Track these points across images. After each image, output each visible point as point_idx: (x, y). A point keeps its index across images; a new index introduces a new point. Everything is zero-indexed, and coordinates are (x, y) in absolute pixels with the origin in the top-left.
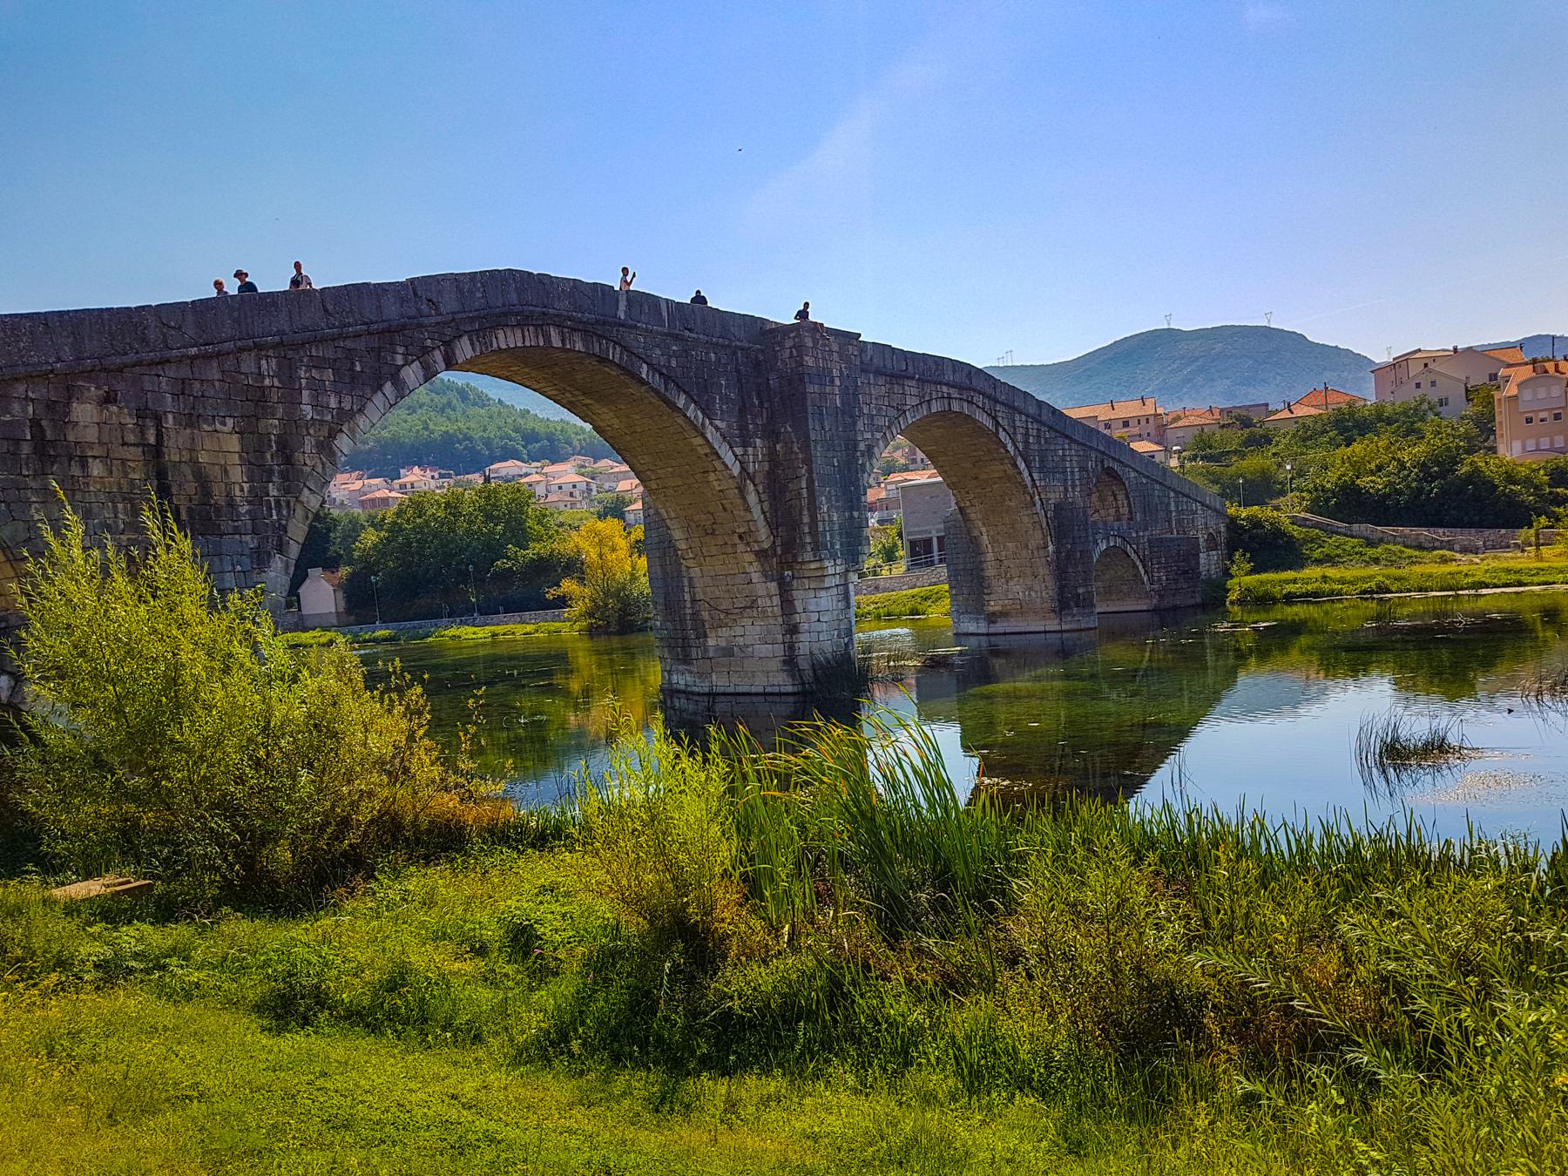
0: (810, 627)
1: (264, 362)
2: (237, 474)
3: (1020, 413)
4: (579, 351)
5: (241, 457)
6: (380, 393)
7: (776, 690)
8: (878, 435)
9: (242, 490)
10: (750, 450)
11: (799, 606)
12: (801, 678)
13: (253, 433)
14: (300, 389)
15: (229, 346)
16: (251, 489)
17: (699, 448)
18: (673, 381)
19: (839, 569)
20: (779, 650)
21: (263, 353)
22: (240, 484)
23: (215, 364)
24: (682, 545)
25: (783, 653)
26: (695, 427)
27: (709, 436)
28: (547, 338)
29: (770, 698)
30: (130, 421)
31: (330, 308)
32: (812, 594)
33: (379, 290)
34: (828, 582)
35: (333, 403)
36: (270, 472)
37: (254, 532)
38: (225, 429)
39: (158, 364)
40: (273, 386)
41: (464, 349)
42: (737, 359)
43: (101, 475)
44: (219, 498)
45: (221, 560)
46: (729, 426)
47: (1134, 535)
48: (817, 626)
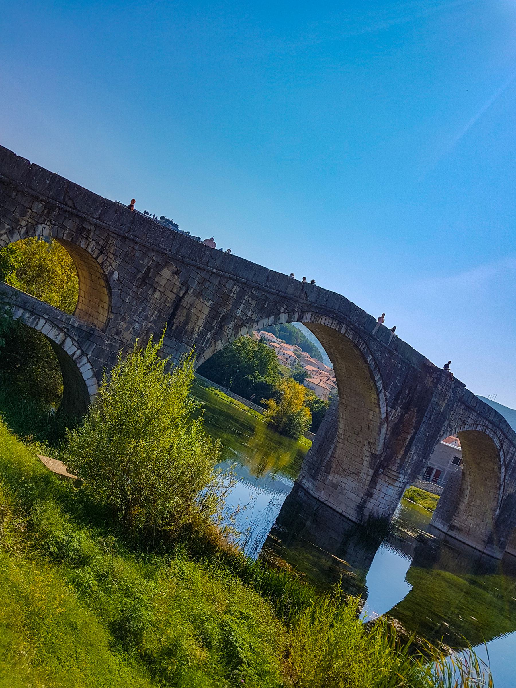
0: (378, 498)
1: (235, 287)
2: (201, 323)
4: (349, 339)
5: (206, 317)
6: (268, 319)
7: (347, 516)
9: (199, 329)
10: (394, 411)
11: (378, 486)
12: (362, 517)
13: (215, 310)
14: (242, 303)
15: (228, 275)
16: (202, 330)
17: (373, 399)
18: (378, 368)
19: (404, 481)
20: (359, 500)
21: (237, 283)
22: (199, 326)
23: (219, 279)
24: (341, 431)
25: (359, 502)
26: (377, 391)
27: (380, 397)
28: (340, 329)
29: (343, 518)
30: (178, 284)
31: (270, 278)
32: (387, 484)
33: (291, 281)
34: (397, 484)
36: (212, 328)
38: (208, 304)
39: (200, 269)
40: (233, 297)
41: (308, 317)
42: (409, 371)
43: (157, 298)
44: (189, 328)
45: (177, 353)
46: (391, 397)
48: (380, 499)
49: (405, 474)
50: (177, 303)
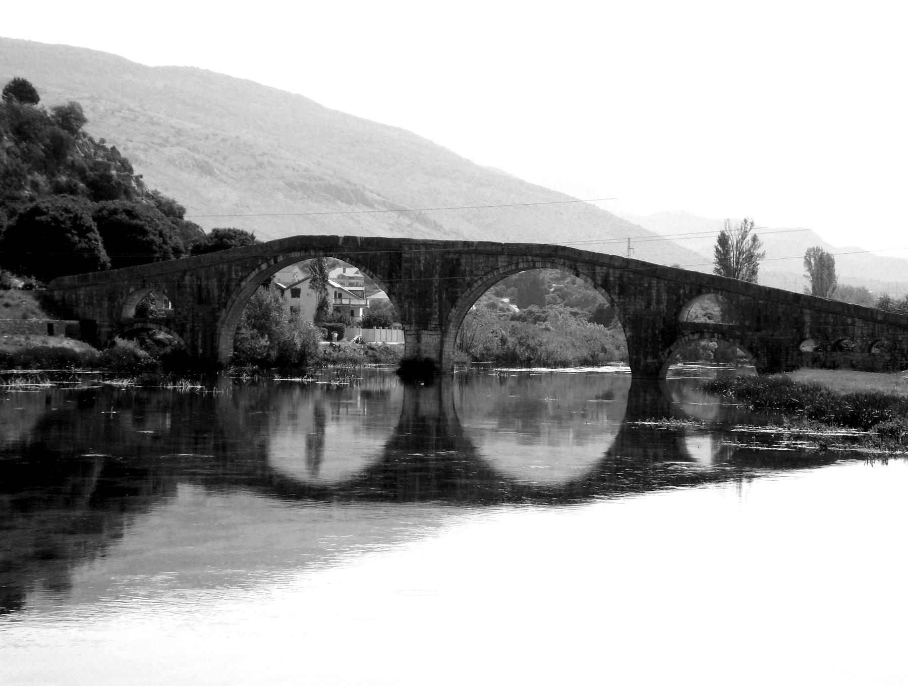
3: (602, 265)
8: (476, 278)
30: (195, 279)
35: (240, 274)
44: (211, 296)
46: (384, 277)
47: (738, 333)
49: (410, 324)
50: (199, 287)
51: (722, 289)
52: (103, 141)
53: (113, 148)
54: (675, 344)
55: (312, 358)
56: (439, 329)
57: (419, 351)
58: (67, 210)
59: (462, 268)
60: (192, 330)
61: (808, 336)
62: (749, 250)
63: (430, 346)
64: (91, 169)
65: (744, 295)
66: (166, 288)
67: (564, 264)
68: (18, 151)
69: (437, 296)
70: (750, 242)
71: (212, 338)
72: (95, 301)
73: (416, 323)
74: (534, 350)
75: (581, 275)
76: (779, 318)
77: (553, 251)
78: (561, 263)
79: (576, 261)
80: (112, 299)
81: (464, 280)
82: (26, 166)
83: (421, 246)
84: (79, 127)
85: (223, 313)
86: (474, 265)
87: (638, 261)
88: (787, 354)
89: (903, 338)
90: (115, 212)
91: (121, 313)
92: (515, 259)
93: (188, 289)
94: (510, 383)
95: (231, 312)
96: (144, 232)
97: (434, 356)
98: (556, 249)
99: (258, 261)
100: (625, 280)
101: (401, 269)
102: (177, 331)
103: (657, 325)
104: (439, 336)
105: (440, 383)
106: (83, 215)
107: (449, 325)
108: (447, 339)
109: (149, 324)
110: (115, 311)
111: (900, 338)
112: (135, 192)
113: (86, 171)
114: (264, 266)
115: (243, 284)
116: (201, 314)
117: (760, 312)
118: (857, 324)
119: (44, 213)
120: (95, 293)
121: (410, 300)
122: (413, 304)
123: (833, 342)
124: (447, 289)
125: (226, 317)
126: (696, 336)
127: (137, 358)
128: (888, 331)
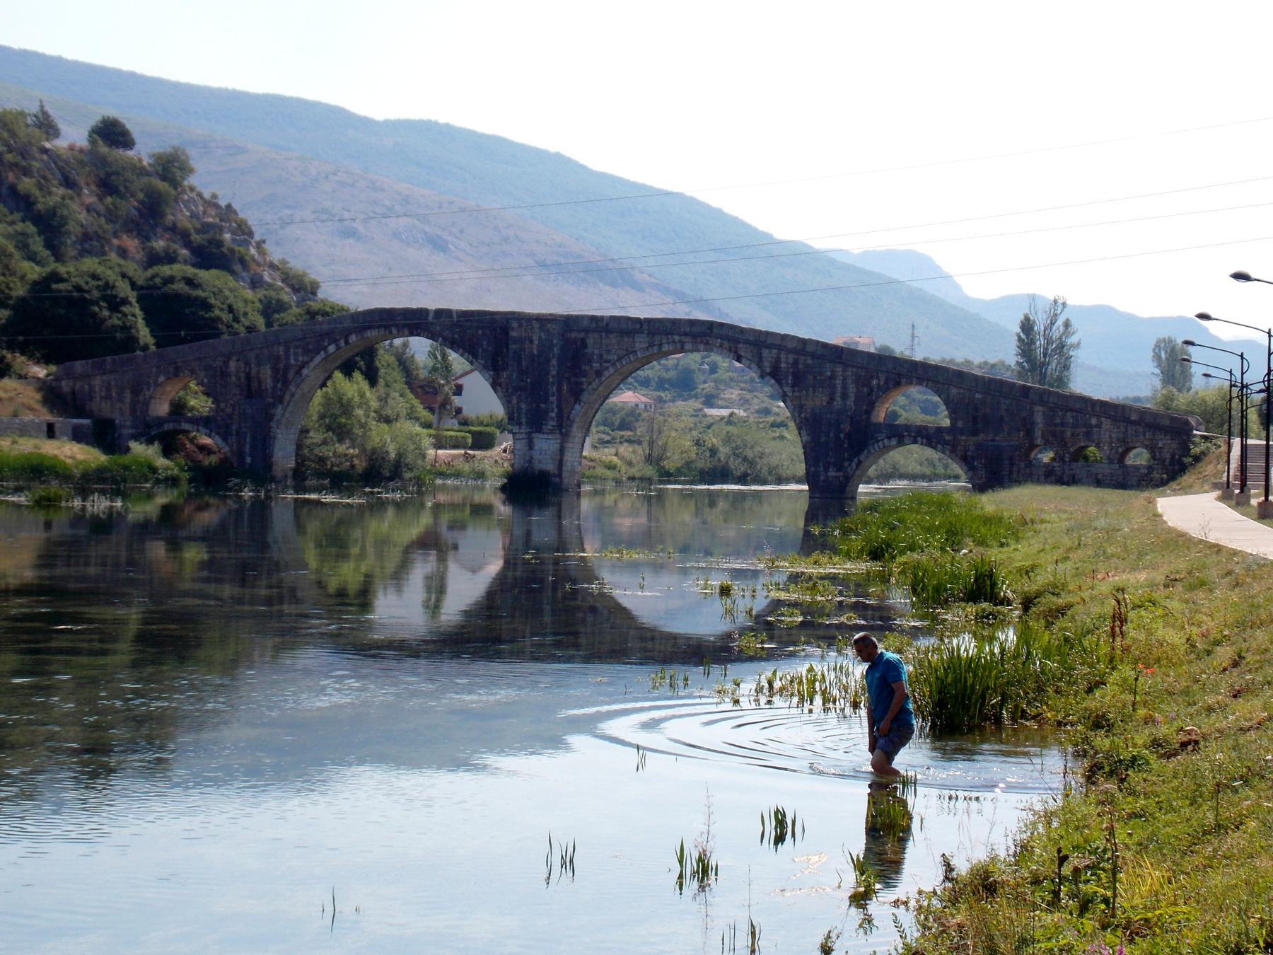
3: (770, 347)
35: (301, 359)
37: (273, 397)
44: (263, 385)
47: (947, 438)
49: (520, 424)
50: (248, 376)
51: (928, 380)
52: (215, 196)
53: (229, 206)
54: (866, 452)
55: (411, 470)
56: (558, 431)
57: (530, 460)
58: (95, 277)
59: (589, 350)
60: (238, 433)
61: (1039, 441)
62: (1060, 338)
63: (546, 454)
64: (198, 232)
65: (955, 387)
66: (205, 377)
67: (721, 346)
68: (101, 208)
69: (555, 388)
70: (1062, 329)
71: (264, 442)
72: (114, 394)
73: (527, 423)
74: (751, 463)
75: (744, 360)
76: (1002, 418)
77: (708, 328)
78: (718, 345)
79: (737, 341)
80: (136, 392)
81: (592, 367)
82: (109, 227)
83: (534, 322)
84: (183, 179)
85: (279, 410)
86: (604, 347)
87: (818, 342)
88: (1012, 465)
89: (1164, 444)
90: (171, 280)
91: (147, 410)
92: (657, 339)
93: (234, 379)
94: (722, 504)
95: (290, 409)
96: (208, 307)
97: (550, 467)
98: (710, 325)
99: (324, 341)
100: (801, 366)
101: (508, 352)
102: (218, 434)
103: (842, 426)
104: (559, 441)
105: (559, 505)
106: (117, 284)
107: (571, 426)
108: (570, 445)
109: (183, 424)
110: (139, 407)
111: (1160, 445)
112: (254, 260)
113: (190, 235)
114: (332, 348)
115: (305, 371)
116: (249, 411)
117: (976, 409)
118: (1104, 426)
119: (62, 280)
120: (113, 383)
121: (519, 393)
122: (523, 398)
123: (1071, 450)
124: (569, 379)
125: (283, 414)
126: (894, 442)
127: (153, 470)
128: (1144, 435)
